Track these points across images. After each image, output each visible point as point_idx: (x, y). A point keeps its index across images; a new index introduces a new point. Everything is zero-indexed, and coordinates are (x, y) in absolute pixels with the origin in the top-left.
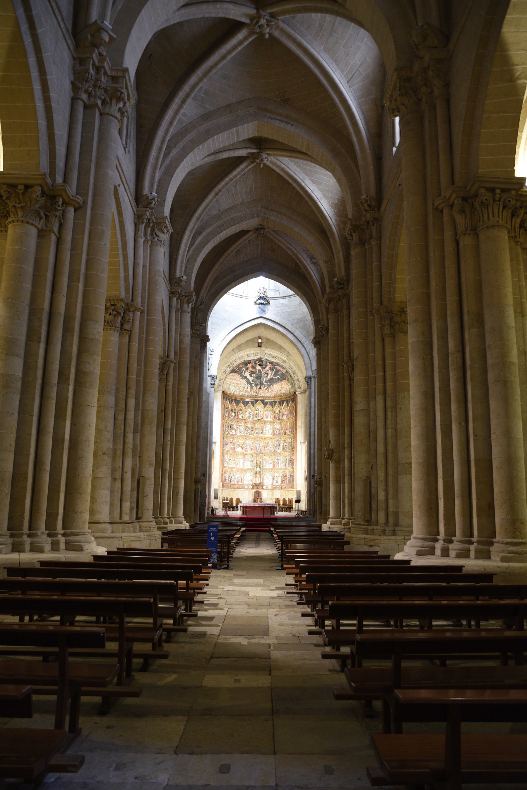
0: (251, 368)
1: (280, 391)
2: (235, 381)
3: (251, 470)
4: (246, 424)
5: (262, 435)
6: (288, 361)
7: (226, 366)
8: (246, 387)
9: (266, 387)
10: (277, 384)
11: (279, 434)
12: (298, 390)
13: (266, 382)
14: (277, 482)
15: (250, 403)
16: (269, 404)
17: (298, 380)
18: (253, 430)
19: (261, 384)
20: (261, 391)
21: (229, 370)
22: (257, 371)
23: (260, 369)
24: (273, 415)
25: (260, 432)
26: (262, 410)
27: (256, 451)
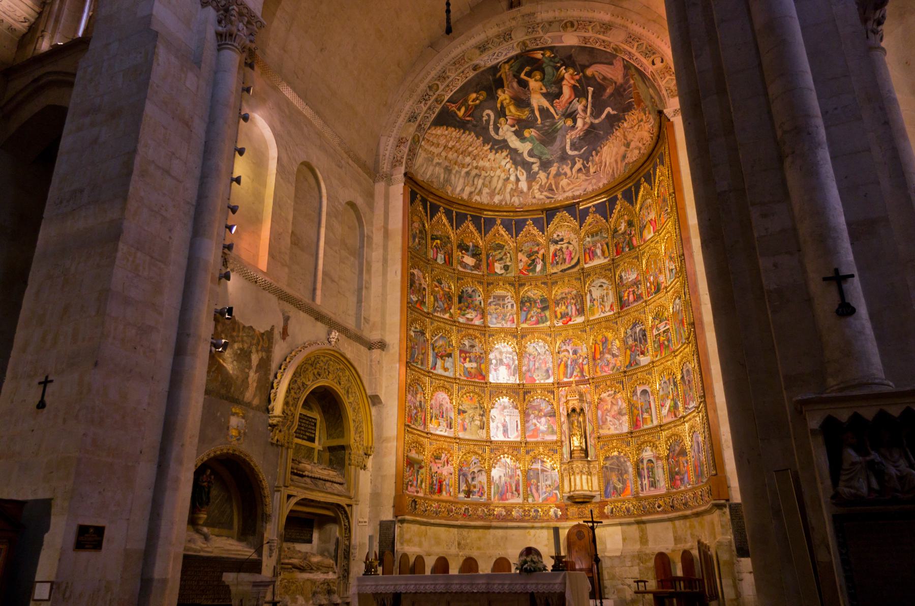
0: (512, 108)
1: (624, 157)
2: (468, 160)
3: (553, 448)
5: (580, 320)
6: (618, 21)
7: (415, 97)
8: (512, 178)
9: (578, 165)
11: (638, 298)
13: (574, 146)
14: (653, 484)
16: (594, 212)
18: (544, 309)
19: (564, 158)
20: (564, 182)
21: (427, 111)
22: (537, 113)
23: (545, 104)
25: (572, 310)
26: (573, 236)
27: (565, 375)
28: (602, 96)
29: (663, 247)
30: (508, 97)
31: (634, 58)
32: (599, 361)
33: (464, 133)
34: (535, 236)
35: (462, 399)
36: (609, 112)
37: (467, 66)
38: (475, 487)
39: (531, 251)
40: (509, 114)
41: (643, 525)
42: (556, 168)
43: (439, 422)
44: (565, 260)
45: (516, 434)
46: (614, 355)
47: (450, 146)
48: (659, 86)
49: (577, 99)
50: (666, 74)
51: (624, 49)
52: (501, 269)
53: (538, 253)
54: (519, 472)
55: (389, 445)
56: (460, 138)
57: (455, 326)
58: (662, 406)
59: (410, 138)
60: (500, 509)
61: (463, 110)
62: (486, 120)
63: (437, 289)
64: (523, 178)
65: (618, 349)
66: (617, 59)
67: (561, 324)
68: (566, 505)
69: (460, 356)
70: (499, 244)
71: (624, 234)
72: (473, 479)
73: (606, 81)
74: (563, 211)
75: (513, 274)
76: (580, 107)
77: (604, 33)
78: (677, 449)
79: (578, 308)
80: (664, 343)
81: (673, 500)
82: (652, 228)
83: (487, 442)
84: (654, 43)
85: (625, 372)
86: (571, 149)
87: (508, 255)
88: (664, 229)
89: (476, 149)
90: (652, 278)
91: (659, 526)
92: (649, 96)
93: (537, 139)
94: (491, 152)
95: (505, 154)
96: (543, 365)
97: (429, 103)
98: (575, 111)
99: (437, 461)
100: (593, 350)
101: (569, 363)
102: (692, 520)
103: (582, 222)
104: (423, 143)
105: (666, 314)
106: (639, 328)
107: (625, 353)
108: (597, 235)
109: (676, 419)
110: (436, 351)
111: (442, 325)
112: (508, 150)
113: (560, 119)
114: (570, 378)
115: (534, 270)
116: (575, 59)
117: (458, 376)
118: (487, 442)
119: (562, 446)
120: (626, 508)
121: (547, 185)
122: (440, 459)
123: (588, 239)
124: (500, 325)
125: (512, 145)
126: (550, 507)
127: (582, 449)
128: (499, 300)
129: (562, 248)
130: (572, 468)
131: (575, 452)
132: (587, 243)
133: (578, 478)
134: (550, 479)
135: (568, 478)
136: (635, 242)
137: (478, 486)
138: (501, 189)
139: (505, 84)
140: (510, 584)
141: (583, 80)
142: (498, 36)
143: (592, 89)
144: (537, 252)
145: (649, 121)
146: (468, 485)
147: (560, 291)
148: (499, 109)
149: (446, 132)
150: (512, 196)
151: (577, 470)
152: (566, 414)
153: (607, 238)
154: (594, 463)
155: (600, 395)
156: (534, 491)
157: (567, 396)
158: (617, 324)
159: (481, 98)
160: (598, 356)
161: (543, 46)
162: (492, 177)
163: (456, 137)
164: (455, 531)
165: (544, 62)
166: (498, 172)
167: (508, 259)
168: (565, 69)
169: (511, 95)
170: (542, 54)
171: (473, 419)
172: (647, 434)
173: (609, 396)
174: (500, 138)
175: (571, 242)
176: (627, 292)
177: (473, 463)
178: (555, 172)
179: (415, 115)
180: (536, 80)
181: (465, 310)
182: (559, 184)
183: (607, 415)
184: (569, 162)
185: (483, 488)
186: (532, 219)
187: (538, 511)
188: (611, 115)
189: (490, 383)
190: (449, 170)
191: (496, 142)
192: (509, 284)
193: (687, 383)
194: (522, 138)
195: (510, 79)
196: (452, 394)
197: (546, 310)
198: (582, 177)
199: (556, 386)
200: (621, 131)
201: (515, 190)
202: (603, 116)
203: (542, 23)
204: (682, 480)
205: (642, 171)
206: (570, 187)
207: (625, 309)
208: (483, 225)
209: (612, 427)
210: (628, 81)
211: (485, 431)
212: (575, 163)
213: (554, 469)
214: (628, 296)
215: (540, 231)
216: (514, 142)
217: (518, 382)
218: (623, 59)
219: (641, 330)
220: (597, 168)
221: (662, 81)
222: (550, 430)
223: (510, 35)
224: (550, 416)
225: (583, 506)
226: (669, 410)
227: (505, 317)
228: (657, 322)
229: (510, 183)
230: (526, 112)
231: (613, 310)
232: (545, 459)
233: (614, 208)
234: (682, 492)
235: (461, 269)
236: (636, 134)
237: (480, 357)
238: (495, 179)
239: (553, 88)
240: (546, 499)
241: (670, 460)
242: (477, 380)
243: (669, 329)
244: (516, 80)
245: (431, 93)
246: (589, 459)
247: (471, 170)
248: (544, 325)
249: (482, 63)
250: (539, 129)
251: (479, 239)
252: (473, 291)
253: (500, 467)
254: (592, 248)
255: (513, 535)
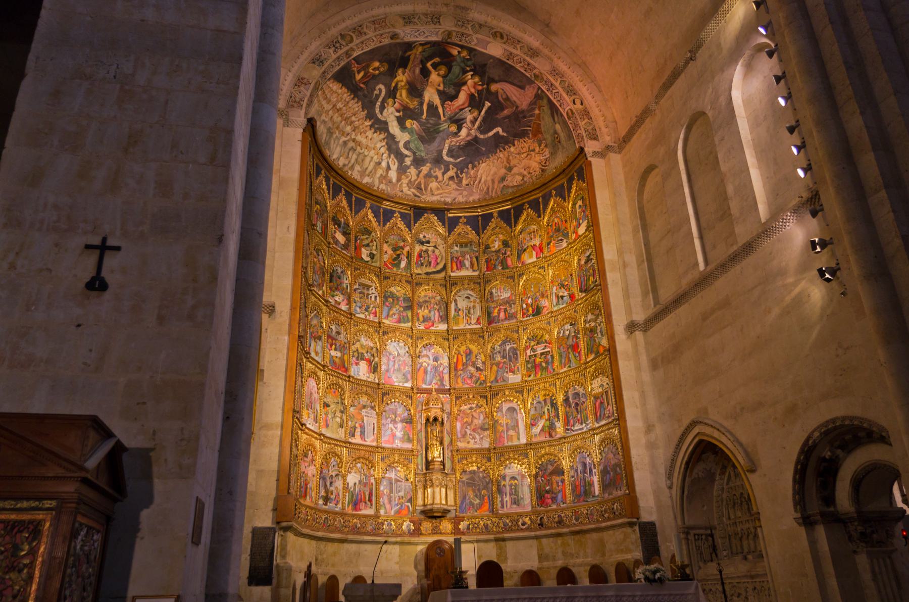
0: (404, 93)
2: (348, 129)
3: (407, 456)
4: (384, 283)
5: (443, 327)
6: (546, 51)
8: (384, 164)
9: (451, 173)
10: (492, 158)
11: (509, 317)
12: (590, 147)
14: (516, 502)
15: (396, 214)
16: (465, 224)
17: (586, 113)
20: (433, 185)
21: (334, 59)
23: (437, 101)
24: (483, 259)
25: (434, 315)
26: (440, 241)
27: (424, 381)
28: (497, 114)
29: (551, 274)
30: (404, 80)
31: (554, 91)
32: (461, 372)
33: (353, 99)
34: (402, 230)
35: (327, 391)
36: (498, 132)
37: (387, 31)
38: (332, 494)
39: (397, 245)
40: (399, 98)
41: (502, 543)
42: (428, 169)
43: (309, 414)
44: (430, 263)
45: (372, 437)
46: (478, 369)
47: (338, 107)
48: (576, 126)
49: (470, 108)
50: (585, 117)
51: (547, 78)
52: (367, 256)
53: (403, 249)
54: (373, 480)
55: (270, 433)
56: (348, 102)
57: (327, 306)
58: (533, 425)
59: (314, 82)
60: (355, 520)
61: (362, 74)
62: (376, 94)
63: (315, 260)
64: (394, 167)
65: (484, 363)
66: (533, 85)
67: (422, 327)
68: (421, 520)
69: (328, 342)
70: (367, 228)
71: (497, 251)
72: (331, 483)
73: (508, 103)
74: (431, 214)
75: (377, 265)
76: (469, 117)
77: (531, 57)
78: (550, 468)
79: (441, 314)
80: (541, 365)
81: (542, 518)
82: (534, 253)
83: (345, 443)
84: (575, 84)
85: (490, 387)
86: (447, 155)
87: (375, 242)
88: (556, 257)
89: (358, 121)
90: (530, 301)
91: (521, 544)
92: (552, 131)
93: (417, 134)
94: (370, 129)
95: (382, 136)
96: (402, 367)
97: (340, 52)
98: (463, 119)
99: (305, 459)
100: (455, 360)
101: (429, 369)
102: (565, 538)
103: (450, 230)
104: (320, 93)
105: (547, 337)
106: (510, 346)
107: (491, 368)
108: (466, 246)
109: (551, 439)
110: (311, 331)
111: (316, 300)
112: (386, 134)
113: (445, 121)
114: (430, 385)
115: (398, 265)
116: (487, 70)
117: (325, 364)
118: (345, 443)
119: (417, 455)
120: (484, 524)
121: (416, 183)
122: (307, 457)
123: (456, 248)
124: (362, 316)
125: (391, 131)
126: (404, 521)
127: (441, 462)
128: (364, 288)
129: (428, 250)
130: (431, 480)
131: (435, 463)
132: (455, 252)
133: (437, 490)
134: (403, 490)
135: (422, 490)
136: (509, 262)
137: (335, 492)
138: (371, 172)
139: (409, 67)
140: (641, 596)
141: (484, 92)
142: (426, 15)
143: (489, 104)
144: (402, 248)
145: (542, 154)
146: (327, 491)
147: (423, 294)
148: (392, 89)
149: (340, 91)
150: (381, 182)
151: (436, 483)
152: (424, 422)
153: (477, 252)
154: (451, 476)
155: (461, 406)
156: (386, 501)
157: (427, 403)
158: (483, 338)
159: (382, 69)
160: (460, 367)
161: (466, 45)
162: (366, 156)
163: (345, 100)
164: (314, 543)
165: (455, 60)
166: (372, 152)
167: (374, 248)
168: (472, 75)
169: (409, 79)
170: (459, 52)
171: (334, 417)
172: (512, 451)
173: (471, 408)
174: (383, 119)
175: (437, 246)
176: (497, 309)
177: (332, 465)
178: (426, 172)
179: (322, 59)
180: (439, 75)
181: (334, 292)
182: (428, 185)
183: (467, 428)
184: (442, 166)
185: (339, 495)
186: (400, 213)
187: (391, 525)
188: (499, 135)
189: (353, 377)
190: (330, 132)
191: (378, 121)
192: (375, 274)
193: (573, 405)
194: (403, 127)
195: (416, 63)
196: (319, 383)
197: (409, 310)
198: (453, 185)
199: (415, 391)
200: (506, 153)
201: (385, 177)
202: (491, 134)
203: (472, 22)
204: (554, 499)
205: (526, 198)
206: (439, 192)
207: (494, 325)
208: (353, 204)
209: (472, 441)
210: (534, 109)
211: (343, 430)
212: (449, 170)
213: (408, 480)
214: (499, 313)
215: (407, 227)
216: (394, 128)
217: (377, 381)
218: (539, 88)
219: (511, 348)
220: (470, 182)
221: (582, 121)
222: (406, 437)
223: (439, 19)
224: (406, 423)
225: (438, 520)
226: (542, 430)
227: (369, 308)
228: (533, 343)
229: (381, 168)
230: (415, 102)
231: (480, 324)
232: (399, 469)
233: (488, 225)
234: (556, 511)
235: (334, 246)
236: (523, 161)
237: (344, 346)
238: (368, 159)
239: (451, 89)
240: (399, 512)
241: (539, 478)
242: (340, 372)
243: (549, 351)
244: (421, 66)
245: (344, 44)
246: (446, 471)
247: (348, 140)
248: (406, 325)
249: (402, 35)
250: (421, 124)
251: (349, 218)
252: (342, 272)
253: (355, 473)
254: (460, 258)
255: (366, 550)
